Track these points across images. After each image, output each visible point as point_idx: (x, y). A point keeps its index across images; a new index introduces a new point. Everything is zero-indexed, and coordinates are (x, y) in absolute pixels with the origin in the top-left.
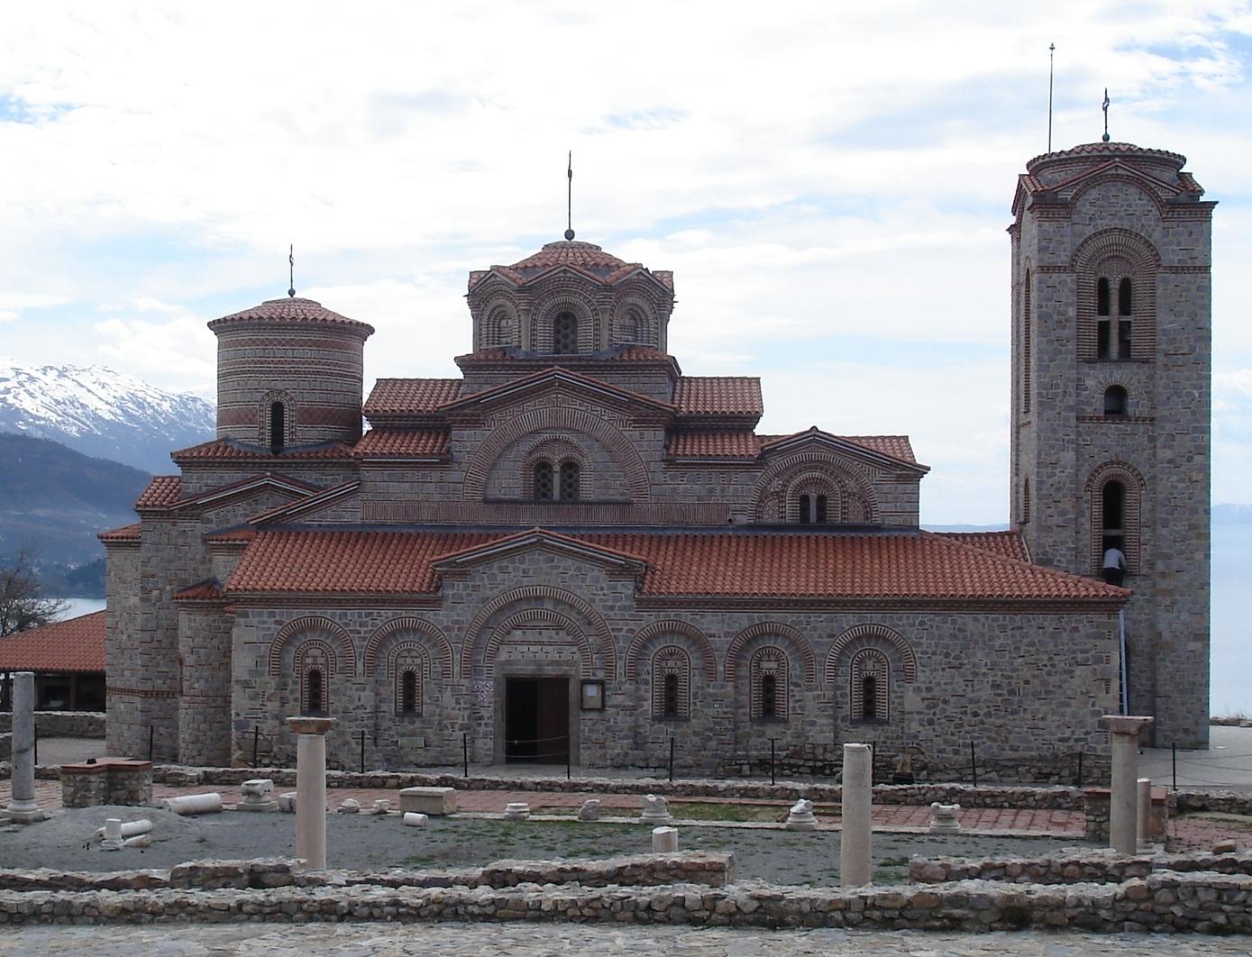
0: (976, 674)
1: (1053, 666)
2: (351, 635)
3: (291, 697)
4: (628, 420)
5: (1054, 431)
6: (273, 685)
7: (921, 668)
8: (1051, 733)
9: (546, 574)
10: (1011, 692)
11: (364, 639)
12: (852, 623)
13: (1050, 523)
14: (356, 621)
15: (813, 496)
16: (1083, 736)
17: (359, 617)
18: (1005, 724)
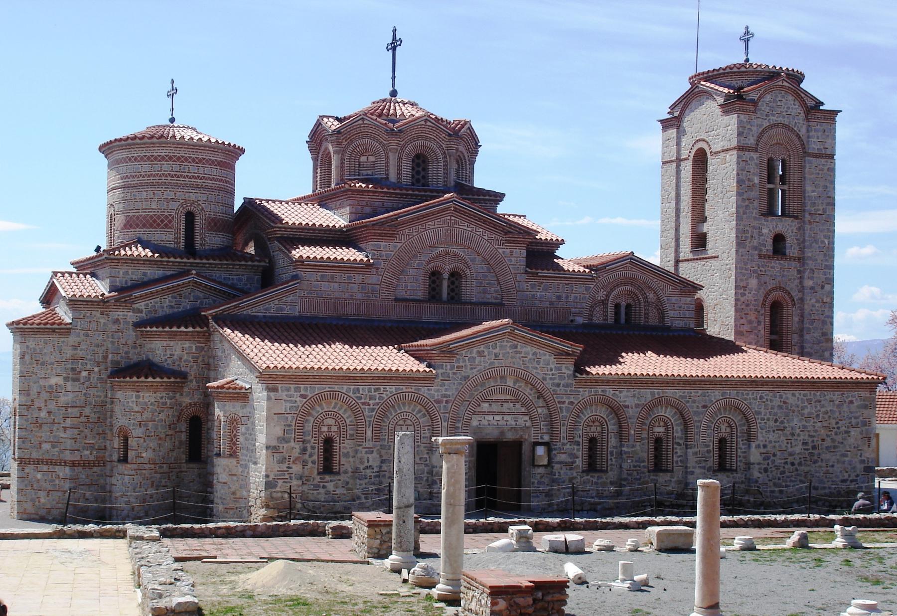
0: (793, 435)
2: (362, 407)
3: (310, 460)
4: (501, 240)
5: (746, 264)
6: (298, 451)
7: (760, 430)
8: (837, 476)
9: (512, 357)
10: (814, 447)
11: (373, 410)
12: (718, 398)
13: (742, 329)
14: (366, 395)
16: (855, 478)
17: (369, 392)
18: (810, 471)
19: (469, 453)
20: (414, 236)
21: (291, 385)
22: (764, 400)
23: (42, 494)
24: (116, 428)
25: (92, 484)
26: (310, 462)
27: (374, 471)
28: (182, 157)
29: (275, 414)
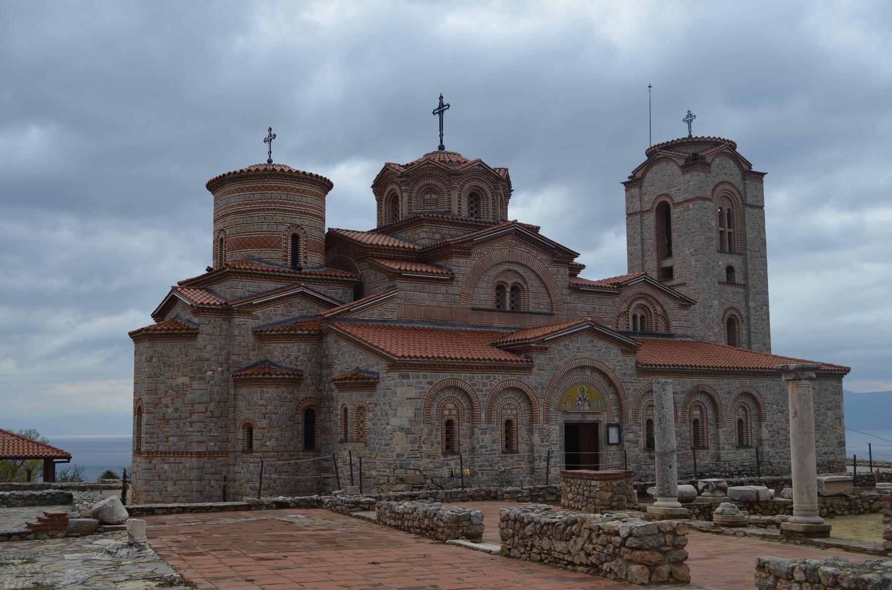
1: (819, 410)
2: (477, 393)
11: (486, 395)
15: (639, 316)
19: (559, 433)
20: (485, 255)
21: (420, 373)
22: (769, 388)
23: (169, 483)
24: (240, 422)
25: (216, 473)
26: (435, 443)
27: (488, 449)
28: (289, 187)
29: (407, 399)
